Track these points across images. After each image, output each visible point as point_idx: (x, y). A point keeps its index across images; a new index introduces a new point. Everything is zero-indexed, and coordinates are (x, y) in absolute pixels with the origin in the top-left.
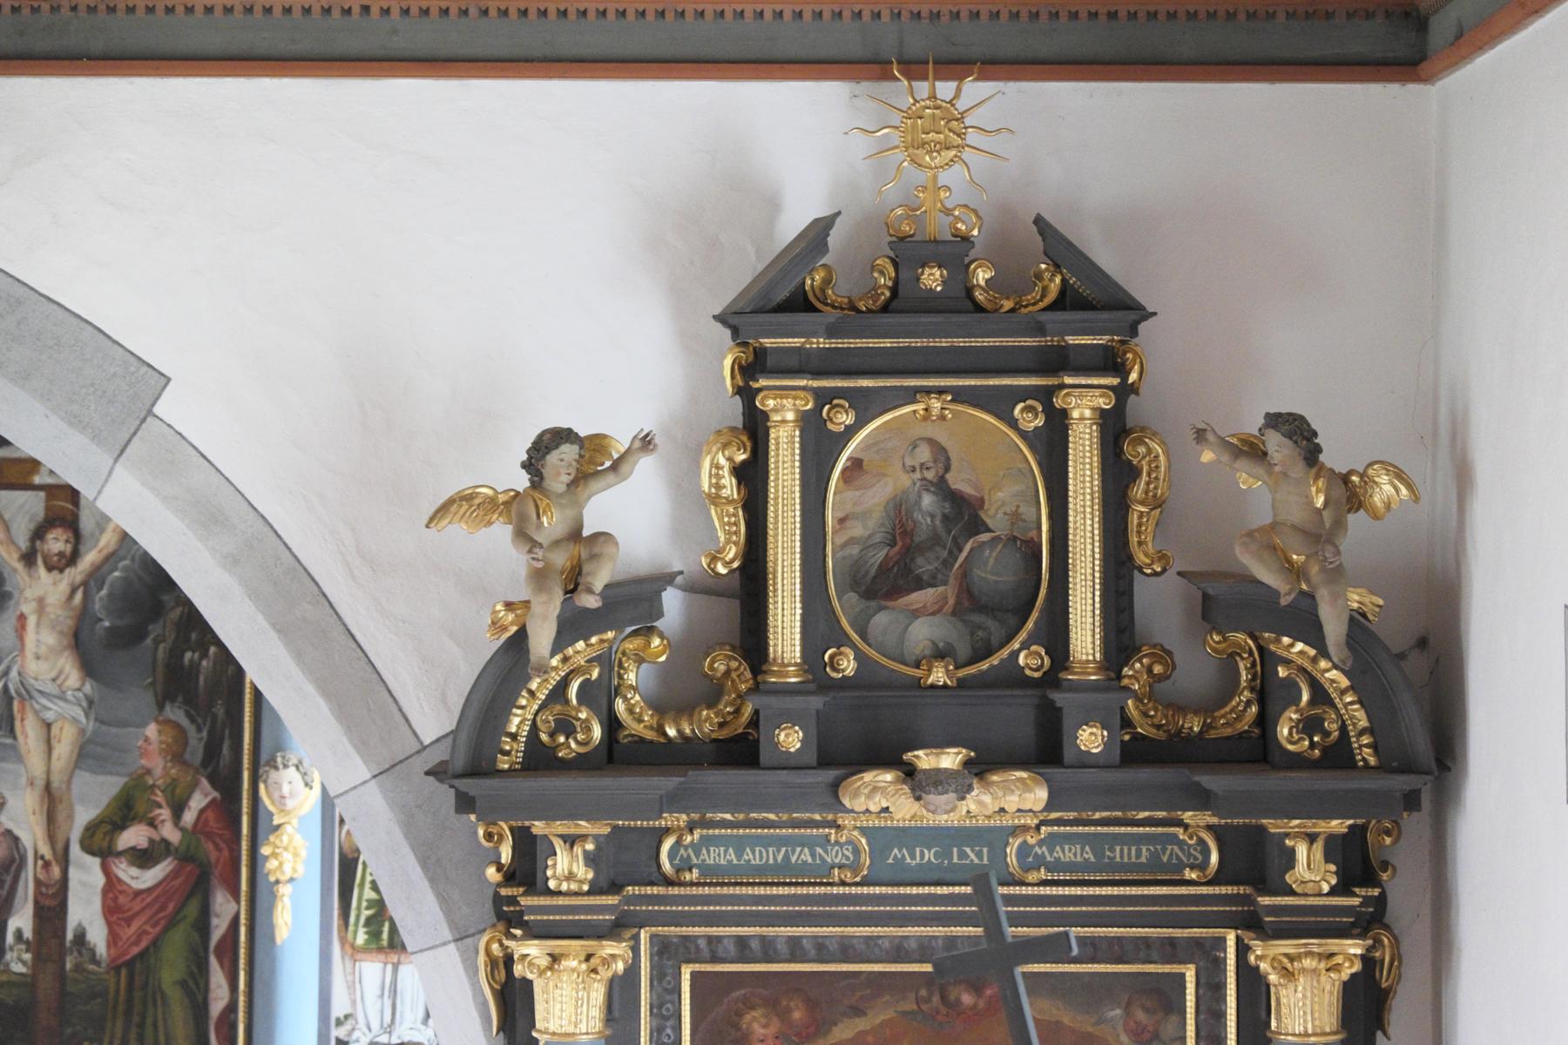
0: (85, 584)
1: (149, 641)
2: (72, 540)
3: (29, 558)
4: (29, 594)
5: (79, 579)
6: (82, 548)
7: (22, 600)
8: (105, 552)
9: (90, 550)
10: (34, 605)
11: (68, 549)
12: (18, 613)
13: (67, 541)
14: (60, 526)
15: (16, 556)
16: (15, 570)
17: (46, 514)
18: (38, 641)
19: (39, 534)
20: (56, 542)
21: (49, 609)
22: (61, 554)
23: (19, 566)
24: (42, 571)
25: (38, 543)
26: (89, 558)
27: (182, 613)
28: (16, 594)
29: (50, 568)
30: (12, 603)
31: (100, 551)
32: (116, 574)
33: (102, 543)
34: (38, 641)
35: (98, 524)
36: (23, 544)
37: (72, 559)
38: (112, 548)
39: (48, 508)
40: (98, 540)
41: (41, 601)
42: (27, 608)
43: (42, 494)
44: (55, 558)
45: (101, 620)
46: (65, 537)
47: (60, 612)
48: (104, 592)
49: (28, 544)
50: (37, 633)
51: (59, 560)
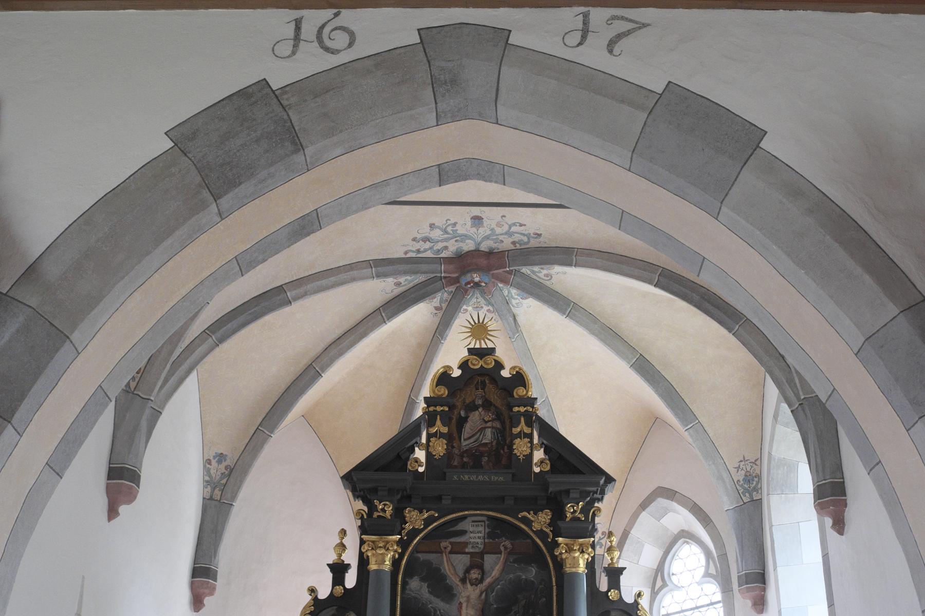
0: (486, 590)
1: (512, 613)
2: (481, 573)
3: (463, 581)
4: (463, 594)
5: (484, 588)
6: (484, 576)
7: (461, 597)
8: (494, 578)
9: (487, 578)
10: (465, 599)
11: (480, 576)
12: (459, 602)
13: (479, 574)
14: (476, 568)
15: (458, 580)
16: (458, 585)
17: (470, 564)
18: (467, 613)
19: (467, 571)
20: (475, 574)
21: (472, 601)
22: (476, 579)
23: (459, 583)
24: (469, 585)
25: (467, 574)
26: (488, 580)
27: (526, 602)
28: (458, 595)
29: (472, 585)
30: (456, 598)
31: (492, 578)
32: (499, 586)
33: (493, 574)
34: (467, 613)
35: (491, 568)
36: (461, 574)
37: (481, 581)
38: (497, 576)
39: (470, 561)
40: (491, 574)
41: (468, 597)
42: (462, 600)
43: (469, 556)
44: (474, 581)
45: (492, 605)
46: (478, 572)
47: (476, 602)
48: (494, 594)
49: (463, 575)
50: (467, 610)
51: (475, 581)
